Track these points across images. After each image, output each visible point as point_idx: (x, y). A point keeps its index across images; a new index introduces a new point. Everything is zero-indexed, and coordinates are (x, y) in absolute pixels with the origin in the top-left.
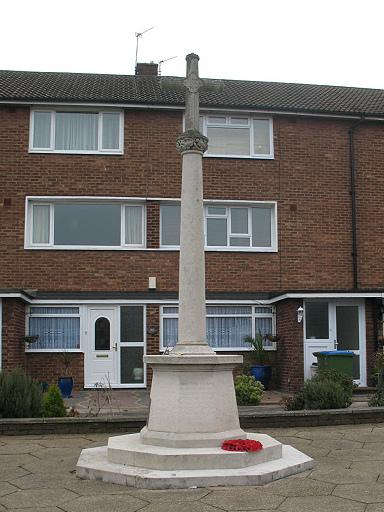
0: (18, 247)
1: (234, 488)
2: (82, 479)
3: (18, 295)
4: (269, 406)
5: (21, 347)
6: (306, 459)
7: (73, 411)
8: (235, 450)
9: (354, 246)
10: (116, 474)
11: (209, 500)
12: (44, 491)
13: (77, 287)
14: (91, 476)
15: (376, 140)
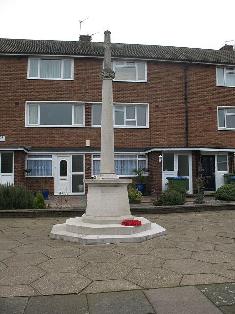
0: (22, 125)
1: (127, 244)
2: (53, 239)
3: (22, 149)
4: (145, 204)
5: (24, 175)
6: (163, 229)
7: (49, 206)
8: (128, 225)
9: (187, 125)
10: (70, 237)
11: (115, 250)
12: (35, 246)
13: (51, 145)
14: (58, 238)
15: (197, 73)
